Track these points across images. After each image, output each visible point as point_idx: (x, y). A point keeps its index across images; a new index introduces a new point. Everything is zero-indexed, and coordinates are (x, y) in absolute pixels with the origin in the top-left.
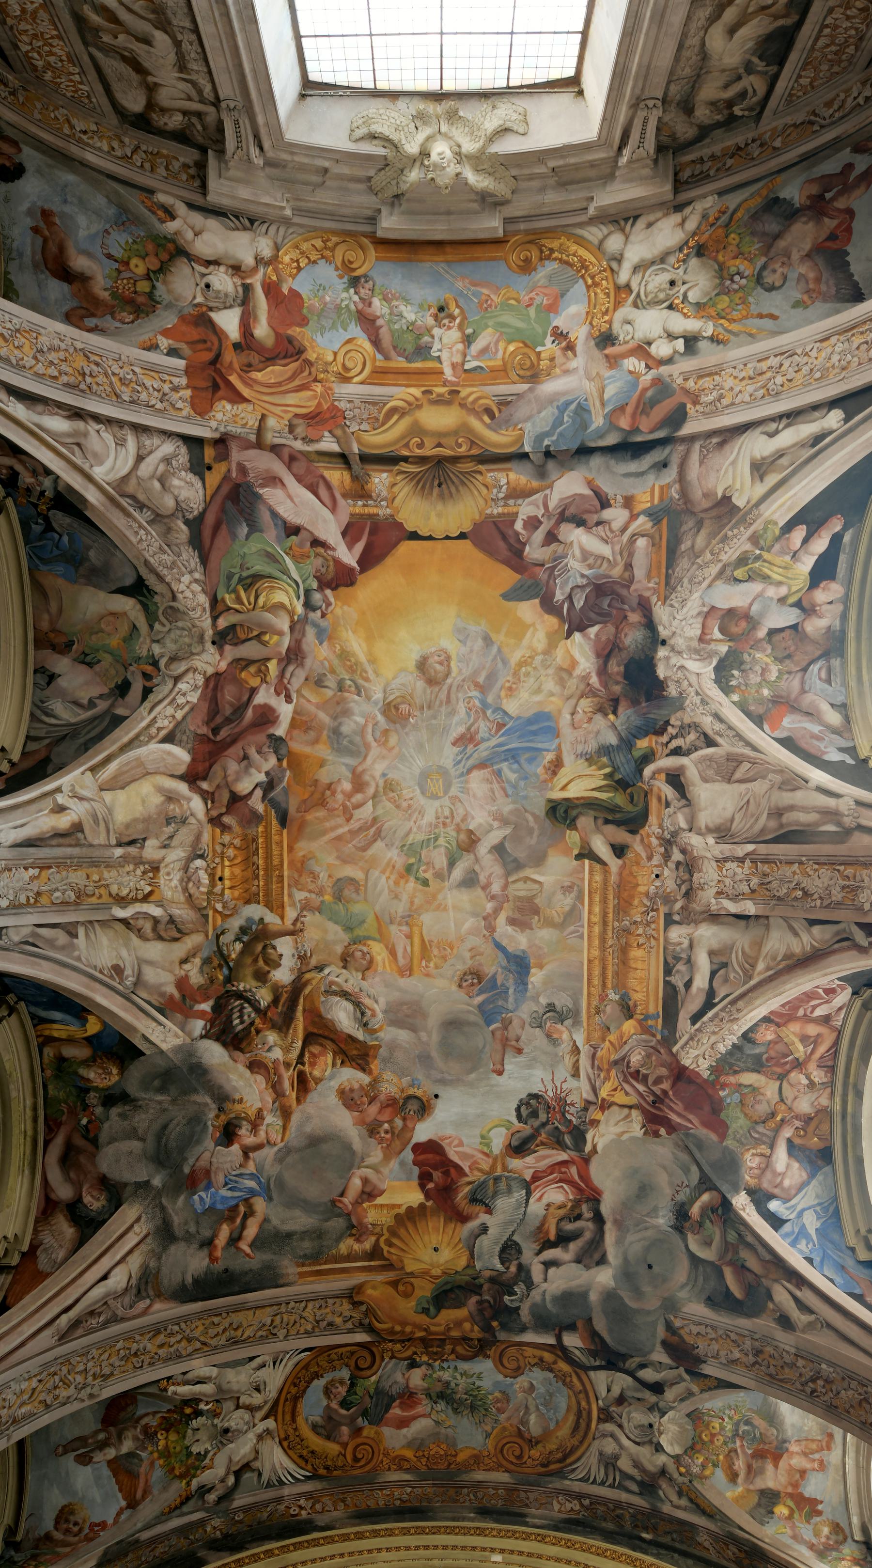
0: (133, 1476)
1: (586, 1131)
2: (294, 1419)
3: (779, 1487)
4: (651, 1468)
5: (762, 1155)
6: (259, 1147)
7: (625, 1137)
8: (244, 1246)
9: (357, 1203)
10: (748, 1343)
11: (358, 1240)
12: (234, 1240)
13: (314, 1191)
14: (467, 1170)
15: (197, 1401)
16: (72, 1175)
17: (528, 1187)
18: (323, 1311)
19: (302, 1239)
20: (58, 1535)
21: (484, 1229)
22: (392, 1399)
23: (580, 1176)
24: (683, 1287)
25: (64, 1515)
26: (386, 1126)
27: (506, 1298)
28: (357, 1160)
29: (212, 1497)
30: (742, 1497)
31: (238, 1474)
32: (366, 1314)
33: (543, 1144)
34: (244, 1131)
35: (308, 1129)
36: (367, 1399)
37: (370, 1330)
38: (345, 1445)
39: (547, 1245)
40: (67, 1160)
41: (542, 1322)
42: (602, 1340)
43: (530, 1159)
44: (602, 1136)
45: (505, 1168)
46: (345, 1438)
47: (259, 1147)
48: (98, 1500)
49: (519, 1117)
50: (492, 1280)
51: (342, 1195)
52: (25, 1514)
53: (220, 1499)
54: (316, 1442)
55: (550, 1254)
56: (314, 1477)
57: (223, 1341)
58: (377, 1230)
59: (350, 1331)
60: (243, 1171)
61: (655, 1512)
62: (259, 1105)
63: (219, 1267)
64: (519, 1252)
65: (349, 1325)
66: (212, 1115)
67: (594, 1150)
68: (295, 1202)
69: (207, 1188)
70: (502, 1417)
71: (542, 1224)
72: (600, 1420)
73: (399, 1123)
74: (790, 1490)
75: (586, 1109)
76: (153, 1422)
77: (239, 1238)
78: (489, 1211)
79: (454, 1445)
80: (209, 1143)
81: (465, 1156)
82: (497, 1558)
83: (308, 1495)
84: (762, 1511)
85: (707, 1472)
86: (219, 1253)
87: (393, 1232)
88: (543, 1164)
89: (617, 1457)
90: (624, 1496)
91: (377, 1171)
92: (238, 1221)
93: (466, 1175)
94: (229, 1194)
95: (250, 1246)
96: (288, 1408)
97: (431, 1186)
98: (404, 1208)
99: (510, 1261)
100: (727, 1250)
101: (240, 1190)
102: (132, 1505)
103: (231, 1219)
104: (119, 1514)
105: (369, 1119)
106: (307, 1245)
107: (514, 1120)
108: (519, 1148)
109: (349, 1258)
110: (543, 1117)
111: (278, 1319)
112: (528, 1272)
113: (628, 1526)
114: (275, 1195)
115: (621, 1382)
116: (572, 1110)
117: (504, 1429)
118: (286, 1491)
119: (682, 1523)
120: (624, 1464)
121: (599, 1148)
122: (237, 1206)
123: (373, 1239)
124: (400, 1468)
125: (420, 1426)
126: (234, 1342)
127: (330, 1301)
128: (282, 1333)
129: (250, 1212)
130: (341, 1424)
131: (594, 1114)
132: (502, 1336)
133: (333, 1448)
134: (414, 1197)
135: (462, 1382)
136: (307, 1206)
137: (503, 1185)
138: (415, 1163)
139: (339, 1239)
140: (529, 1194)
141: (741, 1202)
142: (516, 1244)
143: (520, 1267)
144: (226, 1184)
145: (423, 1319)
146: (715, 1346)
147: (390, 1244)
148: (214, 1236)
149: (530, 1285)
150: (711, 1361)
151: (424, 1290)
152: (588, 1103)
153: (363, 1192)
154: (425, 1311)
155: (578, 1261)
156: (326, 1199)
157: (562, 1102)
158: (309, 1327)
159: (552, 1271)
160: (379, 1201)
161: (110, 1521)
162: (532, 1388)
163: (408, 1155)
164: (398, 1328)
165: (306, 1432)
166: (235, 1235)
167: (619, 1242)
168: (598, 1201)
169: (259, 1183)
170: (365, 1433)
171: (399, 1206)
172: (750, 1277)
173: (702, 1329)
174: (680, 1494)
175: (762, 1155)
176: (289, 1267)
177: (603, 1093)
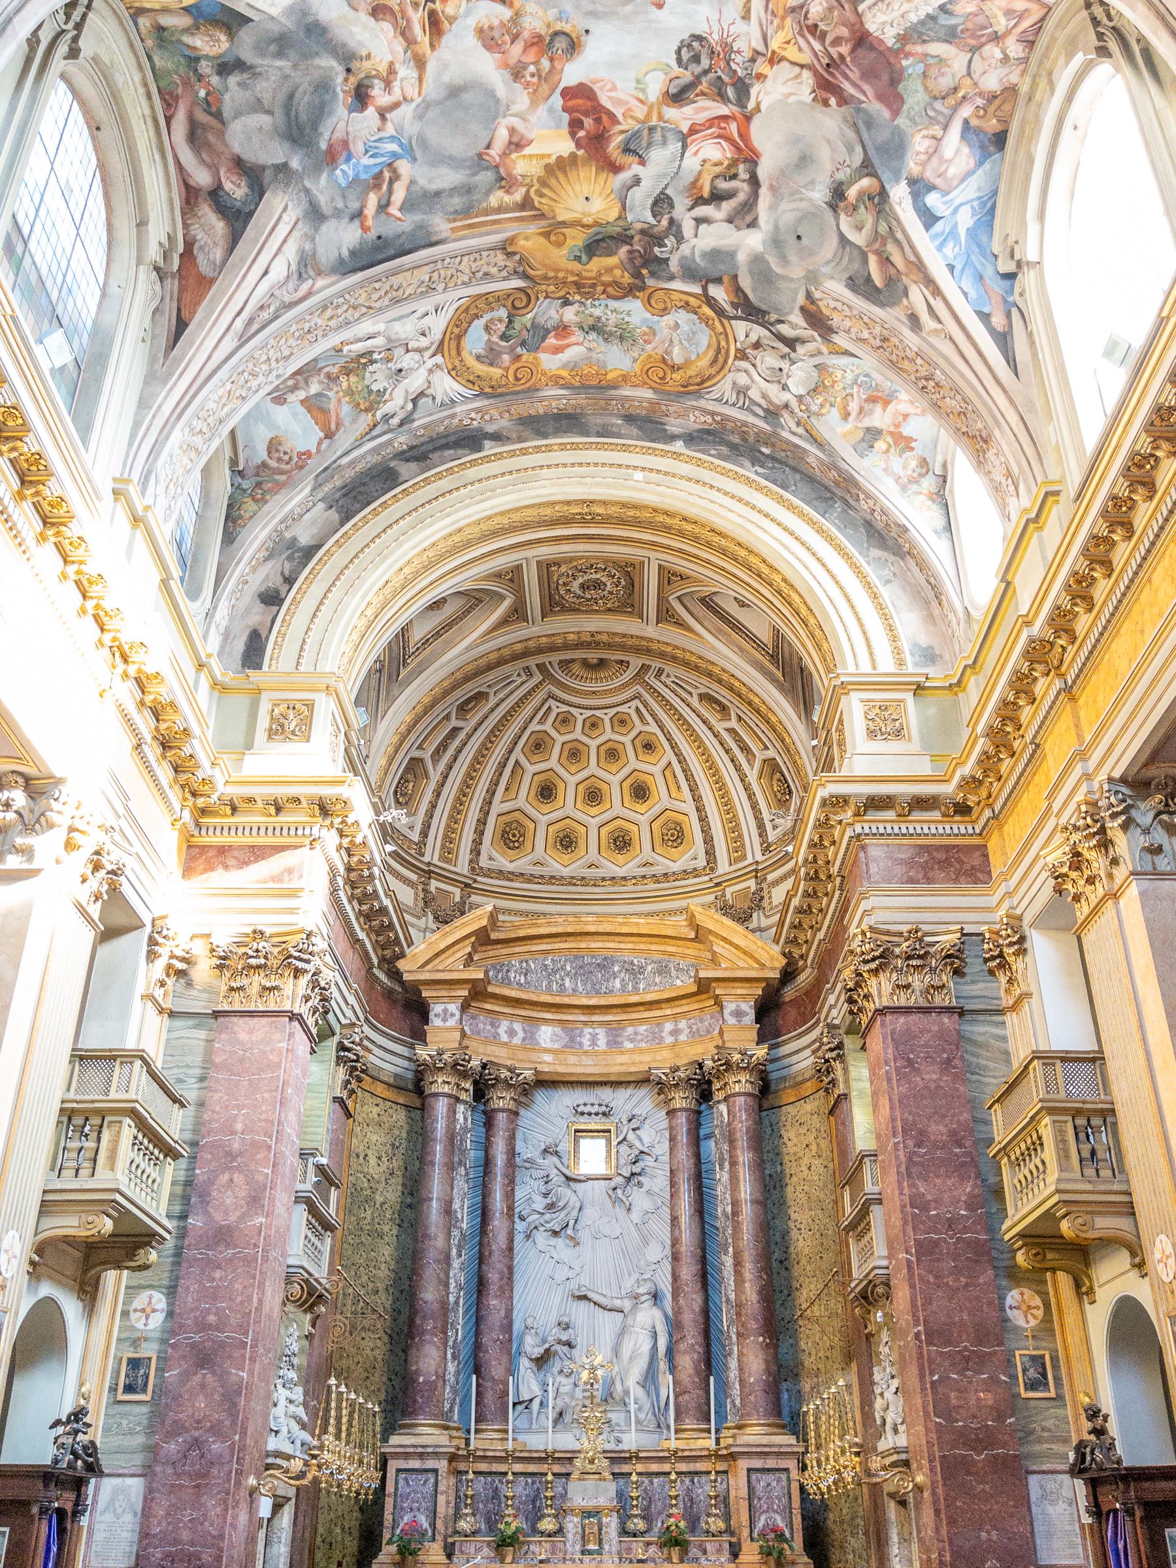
0: (325, 412)
1: (752, 85)
2: (459, 353)
3: (884, 427)
4: (777, 401)
5: (933, 137)
6: (396, 106)
7: (792, 99)
8: (394, 210)
9: (505, 154)
10: (877, 330)
11: (508, 192)
12: (383, 207)
13: (458, 146)
14: (620, 118)
15: (371, 353)
16: (204, 155)
17: (684, 140)
18: (478, 263)
19: (451, 196)
20: (273, 464)
21: (637, 181)
22: (548, 331)
23: (740, 135)
24: (828, 262)
25: (273, 446)
26: (532, 68)
27: (656, 249)
28: (502, 109)
29: (395, 421)
30: (850, 433)
31: (415, 401)
32: (520, 262)
33: (703, 94)
34: (377, 91)
35: (446, 79)
36: (525, 332)
37: (525, 276)
38: (507, 369)
39: (700, 201)
40: (194, 135)
41: (690, 273)
42: (746, 296)
43: (688, 110)
44: (767, 93)
45: (660, 118)
46: (507, 364)
47: (396, 106)
48: (299, 432)
49: (679, 60)
50: (643, 232)
51: (488, 147)
52: (240, 447)
53: (401, 424)
54: (481, 369)
55: (702, 211)
56: (482, 394)
57: (386, 302)
58: (528, 180)
59: (505, 279)
60: (382, 134)
61: (775, 434)
62: (389, 58)
63: (372, 235)
64: (672, 206)
65: (504, 273)
66: (339, 80)
67: (758, 109)
68: (440, 159)
69: (348, 159)
70: (648, 347)
71: (697, 180)
72: (736, 357)
73: (545, 64)
74: (892, 429)
75: (753, 60)
76: (335, 370)
77: (388, 204)
78: (642, 162)
79: (605, 366)
80: (341, 111)
81: (618, 102)
82: (639, 475)
83: (478, 410)
84: (865, 445)
85: (824, 411)
86: (370, 222)
87: (543, 183)
88: (701, 117)
89: (748, 388)
90: (751, 419)
91: (524, 120)
92: (385, 187)
93: (619, 123)
94: (372, 161)
95: (400, 210)
96: (453, 344)
97: (581, 134)
98: (554, 158)
99: (662, 215)
100: (875, 240)
101: (382, 155)
102: (329, 435)
103: (377, 186)
104: (319, 444)
105: (512, 61)
106: (457, 202)
107: (674, 64)
108: (678, 97)
109: (500, 210)
110: (705, 62)
111: (436, 275)
112: (680, 226)
113: (751, 439)
114: (418, 155)
115: (757, 332)
116: (739, 59)
117: (650, 356)
118: (458, 409)
119: (796, 446)
120: (754, 394)
121: (763, 107)
122: (381, 172)
123: (523, 190)
124: (557, 383)
125: (573, 353)
126: (396, 301)
127: (485, 254)
128: (440, 287)
129: (395, 177)
130: (501, 353)
131: (761, 67)
132: (650, 282)
133: (496, 372)
134: (565, 146)
135: (613, 319)
136: (453, 162)
137: (657, 136)
138: (564, 110)
139: (488, 192)
140: (684, 147)
141: (899, 194)
142: (669, 197)
143: (672, 221)
144: (367, 151)
145: (576, 266)
146: (848, 323)
147: (542, 195)
148: (363, 207)
149: (680, 238)
150: (842, 334)
151: (577, 239)
152: (758, 53)
153: (510, 143)
154: (578, 258)
155: (730, 221)
156: (472, 153)
157: (728, 48)
158: (466, 279)
159: (703, 227)
160: (527, 151)
161: (314, 450)
162: (677, 326)
163: (557, 101)
164: (551, 274)
165: (470, 361)
166: (384, 202)
167: (773, 208)
168: (756, 164)
169: (401, 145)
170: (524, 358)
171: (549, 156)
172: (893, 271)
173: (839, 306)
174: (798, 424)
175: (933, 137)
176: (441, 225)
177: (774, 45)
